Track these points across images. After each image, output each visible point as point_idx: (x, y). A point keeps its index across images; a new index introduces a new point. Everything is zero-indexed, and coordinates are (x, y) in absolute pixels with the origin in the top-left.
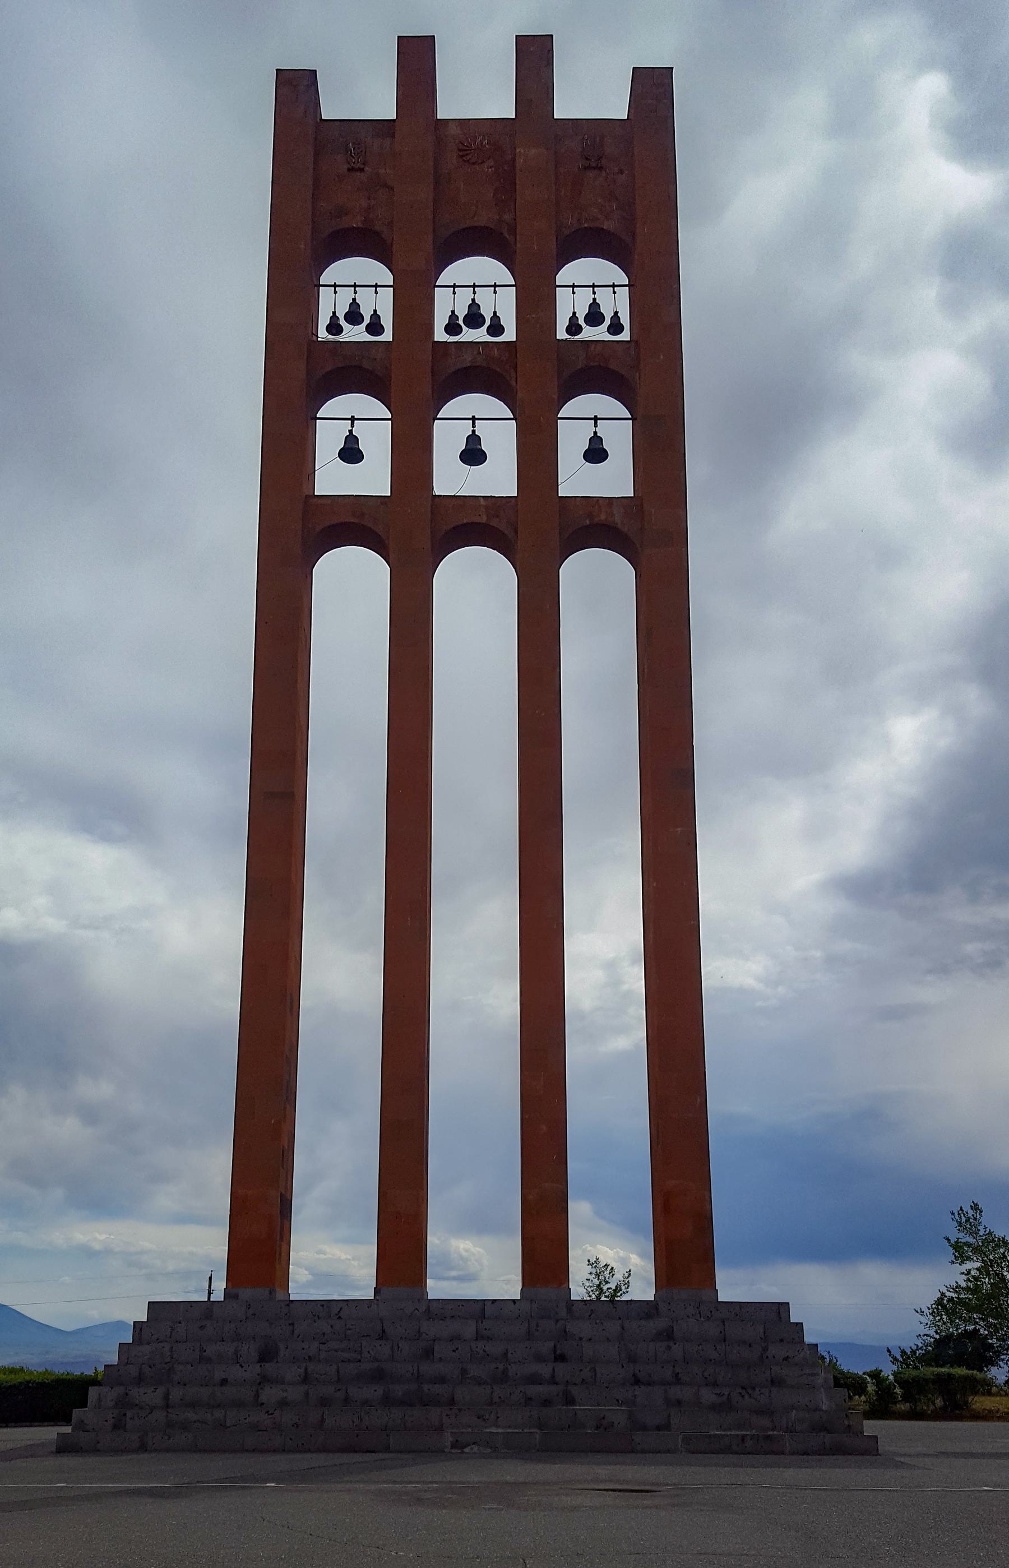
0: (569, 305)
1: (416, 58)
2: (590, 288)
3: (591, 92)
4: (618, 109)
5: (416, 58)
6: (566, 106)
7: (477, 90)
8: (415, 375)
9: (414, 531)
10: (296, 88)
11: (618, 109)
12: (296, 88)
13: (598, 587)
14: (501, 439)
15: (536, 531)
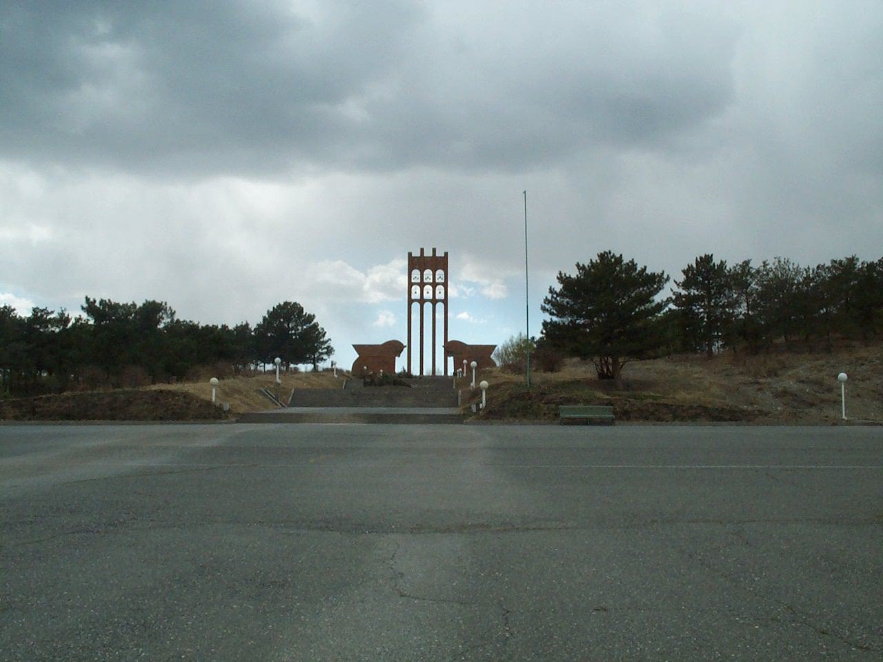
0: (437, 277)
1: (422, 250)
2: (440, 273)
3: (440, 254)
4: (443, 255)
5: (422, 250)
6: (437, 255)
7: (428, 253)
8: (422, 285)
9: (422, 301)
10: (410, 254)
11: (443, 255)
12: (410, 254)
13: (440, 306)
14: (431, 293)
15: (434, 301)
